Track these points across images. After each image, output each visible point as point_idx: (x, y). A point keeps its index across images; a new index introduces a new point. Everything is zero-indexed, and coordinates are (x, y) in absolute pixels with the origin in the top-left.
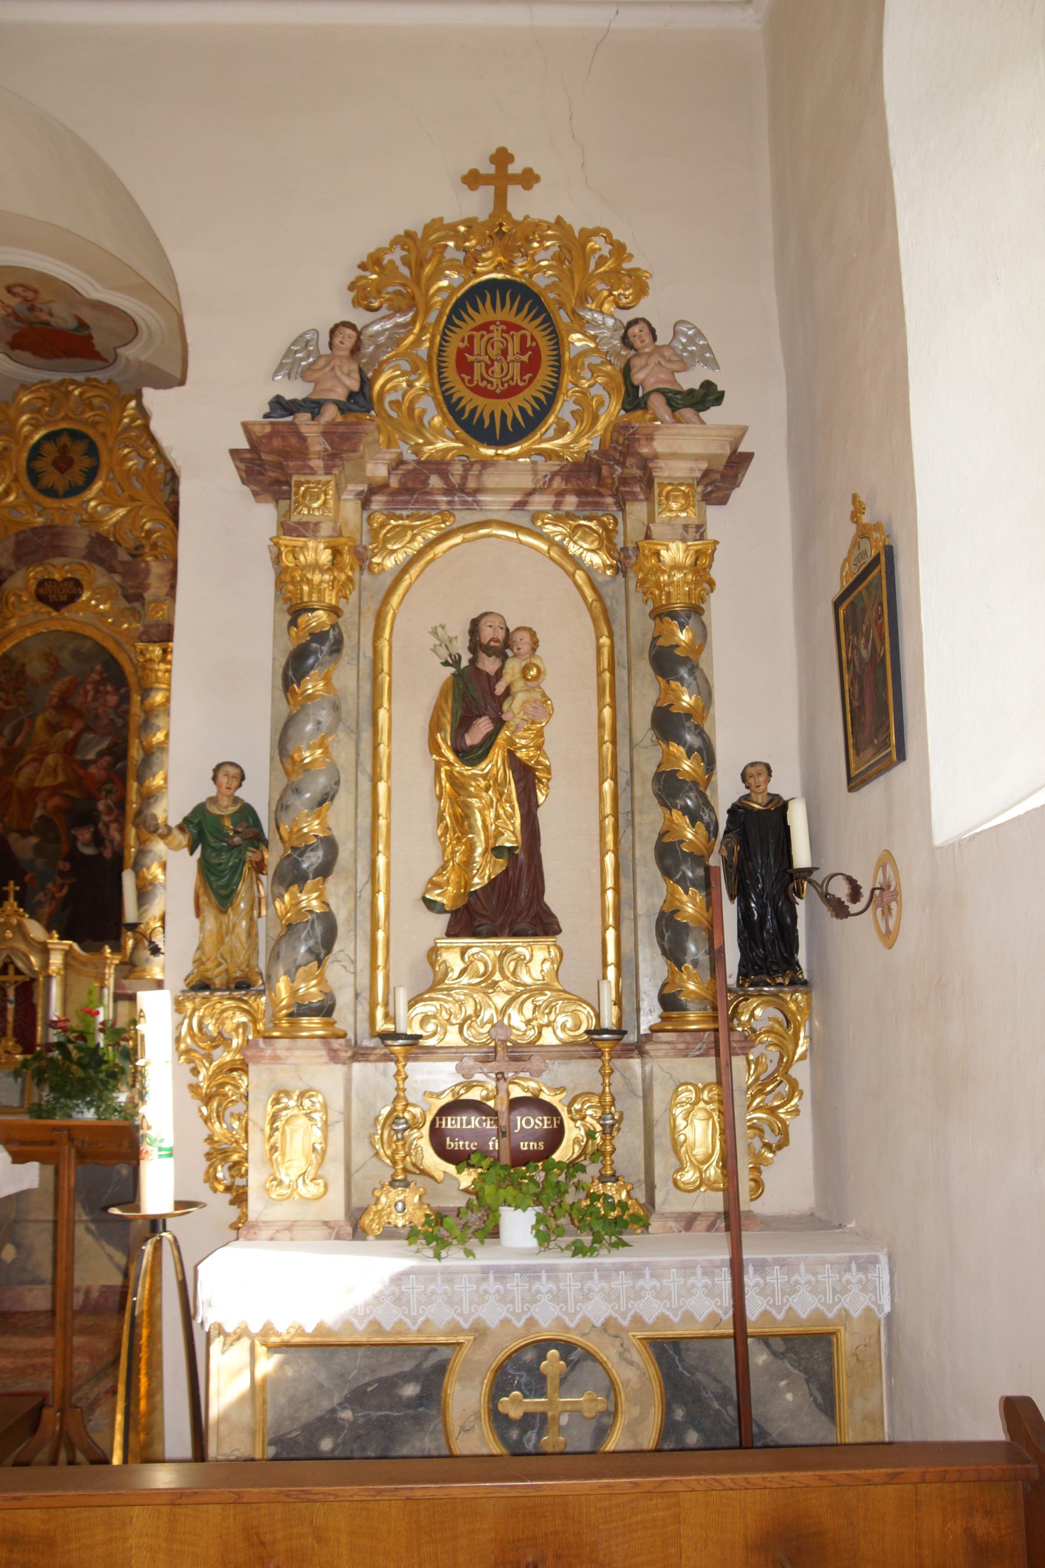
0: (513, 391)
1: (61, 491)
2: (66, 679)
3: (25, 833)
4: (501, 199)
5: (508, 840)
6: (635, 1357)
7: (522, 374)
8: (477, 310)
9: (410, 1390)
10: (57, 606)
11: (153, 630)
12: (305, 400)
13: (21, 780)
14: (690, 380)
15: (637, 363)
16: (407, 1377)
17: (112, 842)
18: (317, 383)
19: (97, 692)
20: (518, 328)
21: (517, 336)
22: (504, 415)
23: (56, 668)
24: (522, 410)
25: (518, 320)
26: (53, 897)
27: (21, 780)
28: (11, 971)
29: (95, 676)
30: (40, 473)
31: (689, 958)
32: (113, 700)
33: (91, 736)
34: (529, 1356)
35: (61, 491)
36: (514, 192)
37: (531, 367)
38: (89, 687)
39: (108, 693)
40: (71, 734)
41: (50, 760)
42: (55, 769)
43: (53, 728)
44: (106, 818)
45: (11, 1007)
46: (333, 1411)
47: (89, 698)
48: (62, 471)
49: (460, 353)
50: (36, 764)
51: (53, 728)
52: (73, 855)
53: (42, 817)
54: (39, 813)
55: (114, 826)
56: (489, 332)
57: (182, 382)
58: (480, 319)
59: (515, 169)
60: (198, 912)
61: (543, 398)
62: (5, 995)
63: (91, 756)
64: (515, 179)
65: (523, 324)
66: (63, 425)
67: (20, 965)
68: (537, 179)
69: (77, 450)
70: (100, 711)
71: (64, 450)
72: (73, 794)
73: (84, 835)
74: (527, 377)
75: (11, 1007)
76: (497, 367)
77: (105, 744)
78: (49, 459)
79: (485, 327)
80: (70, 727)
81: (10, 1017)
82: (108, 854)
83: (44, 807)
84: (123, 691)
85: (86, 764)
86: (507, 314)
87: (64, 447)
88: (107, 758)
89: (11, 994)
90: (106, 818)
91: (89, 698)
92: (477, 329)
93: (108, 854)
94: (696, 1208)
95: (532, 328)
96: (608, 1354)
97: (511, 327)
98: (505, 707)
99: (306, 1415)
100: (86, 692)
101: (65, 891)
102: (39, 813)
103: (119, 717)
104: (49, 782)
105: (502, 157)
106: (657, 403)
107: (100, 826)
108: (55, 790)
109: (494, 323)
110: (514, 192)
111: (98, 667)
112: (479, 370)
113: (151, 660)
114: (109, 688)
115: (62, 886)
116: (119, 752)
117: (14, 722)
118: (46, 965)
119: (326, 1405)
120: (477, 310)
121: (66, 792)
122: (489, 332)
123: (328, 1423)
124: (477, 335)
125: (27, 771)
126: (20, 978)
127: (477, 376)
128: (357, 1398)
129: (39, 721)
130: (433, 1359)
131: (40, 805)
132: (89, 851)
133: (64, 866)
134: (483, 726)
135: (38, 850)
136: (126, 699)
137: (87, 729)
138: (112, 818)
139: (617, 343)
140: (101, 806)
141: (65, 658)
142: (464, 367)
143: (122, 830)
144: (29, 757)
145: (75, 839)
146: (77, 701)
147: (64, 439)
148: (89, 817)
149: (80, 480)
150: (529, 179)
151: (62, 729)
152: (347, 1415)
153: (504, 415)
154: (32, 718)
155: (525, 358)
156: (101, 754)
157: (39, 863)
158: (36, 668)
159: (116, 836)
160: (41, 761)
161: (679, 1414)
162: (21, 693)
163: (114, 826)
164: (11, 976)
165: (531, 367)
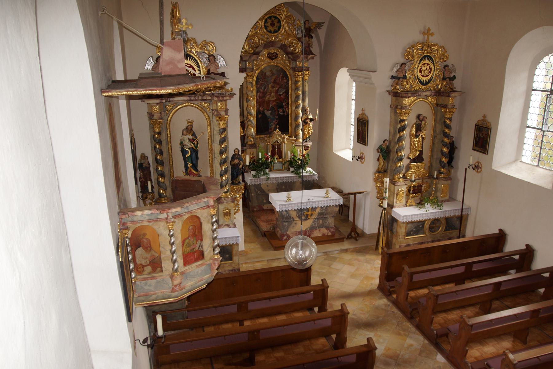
0: (427, 76)
1: (272, 32)
2: (275, 76)
3: (268, 110)
4: (428, 38)
5: (420, 149)
6: (444, 220)
7: (429, 73)
8: (423, 61)
9: (421, 226)
10: (272, 59)
11: (299, 69)
12: (397, 77)
13: (267, 99)
14: (452, 76)
15: (445, 72)
16: (420, 225)
17: (286, 112)
18: (398, 74)
19: (282, 79)
20: (429, 64)
21: (429, 66)
22: (425, 80)
23: (273, 74)
24: (428, 79)
25: (429, 63)
26: (275, 124)
27: (267, 99)
28: (276, 142)
29: (281, 76)
30: (267, 27)
31: (446, 167)
32: (285, 81)
33: (281, 89)
34: (433, 221)
35: (272, 32)
36: (430, 36)
37: (430, 72)
38: (280, 78)
39: (284, 79)
40: (277, 88)
41: (273, 94)
42: (274, 96)
43: (273, 87)
44: (285, 107)
45: (277, 149)
46: (413, 229)
47: (280, 80)
48: (273, 27)
49: (421, 69)
50: (270, 95)
51: (273, 87)
52: (278, 115)
53: (271, 107)
54: (271, 106)
55: (287, 108)
56: (425, 65)
57: (375, 72)
58: (424, 62)
59: (431, 32)
60: (378, 160)
61: (431, 77)
62: (275, 147)
63: (281, 93)
64: (430, 34)
65: (430, 64)
66: (272, 15)
67: (279, 142)
68: (434, 35)
69: (276, 22)
70: (283, 83)
71: (273, 21)
72: (278, 102)
73: (281, 110)
74: (429, 74)
75: (277, 149)
76: (425, 72)
77: (284, 91)
78: (269, 23)
79: (424, 64)
80: (277, 87)
81: (276, 151)
82: (286, 114)
83: (272, 105)
84: (287, 79)
85: (280, 95)
86: (427, 62)
87: (273, 20)
88: (285, 94)
89: (276, 147)
90: (285, 107)
91: (280, 80)
92: (423, 64)
93: (286, 114)
94: (443, 199)
95: (431, 65)
96: (442, 220)
97: (428, 64)
98: (422, 129)
99: (410, 230)
100: (280, 79)
101: (277, 122)
102: (271, 106)
103: (287, 85)
104: (273, 99)
105: (429, 30)
106: (448, 80)
107: (284, 108)
108: (274, 101)
109: (425, 63)
110: (430, 36)
111: (282, 73)
112: (423, 72)
113: (299, 76)
114: (284, 78)
115: (276, 122)
116: (287, 92)
117: (264, 86)
118: (284, 141)
119: (412, 229)
120: (423, 61)
121: (276, 101)
122: (425, 65)
123: (412, 231)
124: (423, 66)
125: (268, 97)
126: (278, 144)
127: (422, 73)
128: (415, 228)
129: (270, 85)
130: (424, 223)
131: (271, 104)
132: (282, 114)
133: (277, 117)
134: (419, 132)
135: (271, 114)
136: (288, 81)
137: (280, 87)
138: (286, 107)
139: (443, 69)
140: (284, 104)
141: (274, 71)
142: (421, 72)
143: (288, 109)
144: (268, 94)
145: (279, 111)
146: (278, 81)
147: (273, 18)
148: (281, 107)
149: (277, 29)
150: (432, 34)
151: (275, 87)
152: (414, 230)
153: (425, 80)
154: (268, 85)
155: (429, 70)
156: (283, 93)
157: (271, 116)
158: (268, 74)
159: (287, 111)
160: (271, 95)
161: (447, 226)
162: (265, 79)
163: (287, 108)
164: (276, 143)
165: (430, 72)
